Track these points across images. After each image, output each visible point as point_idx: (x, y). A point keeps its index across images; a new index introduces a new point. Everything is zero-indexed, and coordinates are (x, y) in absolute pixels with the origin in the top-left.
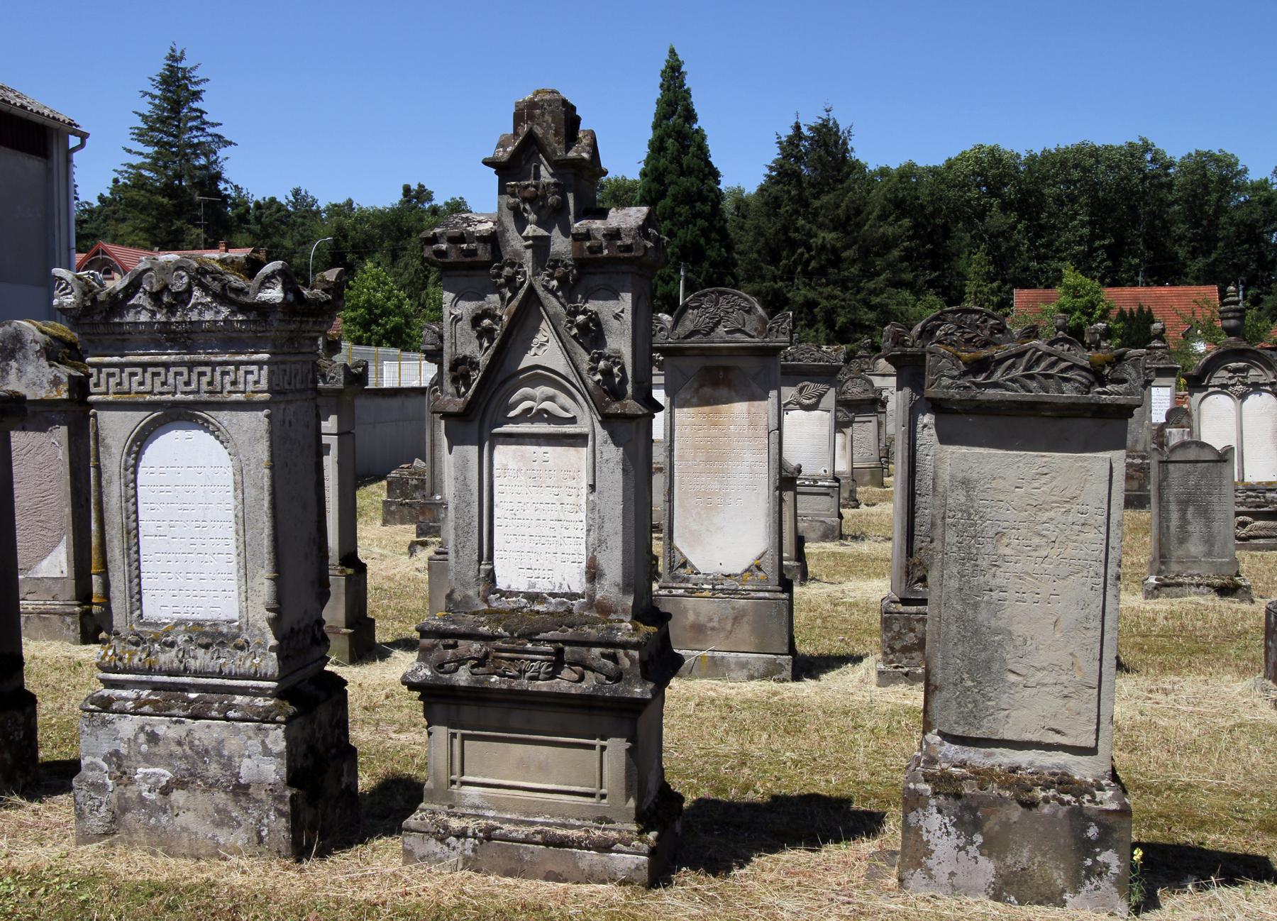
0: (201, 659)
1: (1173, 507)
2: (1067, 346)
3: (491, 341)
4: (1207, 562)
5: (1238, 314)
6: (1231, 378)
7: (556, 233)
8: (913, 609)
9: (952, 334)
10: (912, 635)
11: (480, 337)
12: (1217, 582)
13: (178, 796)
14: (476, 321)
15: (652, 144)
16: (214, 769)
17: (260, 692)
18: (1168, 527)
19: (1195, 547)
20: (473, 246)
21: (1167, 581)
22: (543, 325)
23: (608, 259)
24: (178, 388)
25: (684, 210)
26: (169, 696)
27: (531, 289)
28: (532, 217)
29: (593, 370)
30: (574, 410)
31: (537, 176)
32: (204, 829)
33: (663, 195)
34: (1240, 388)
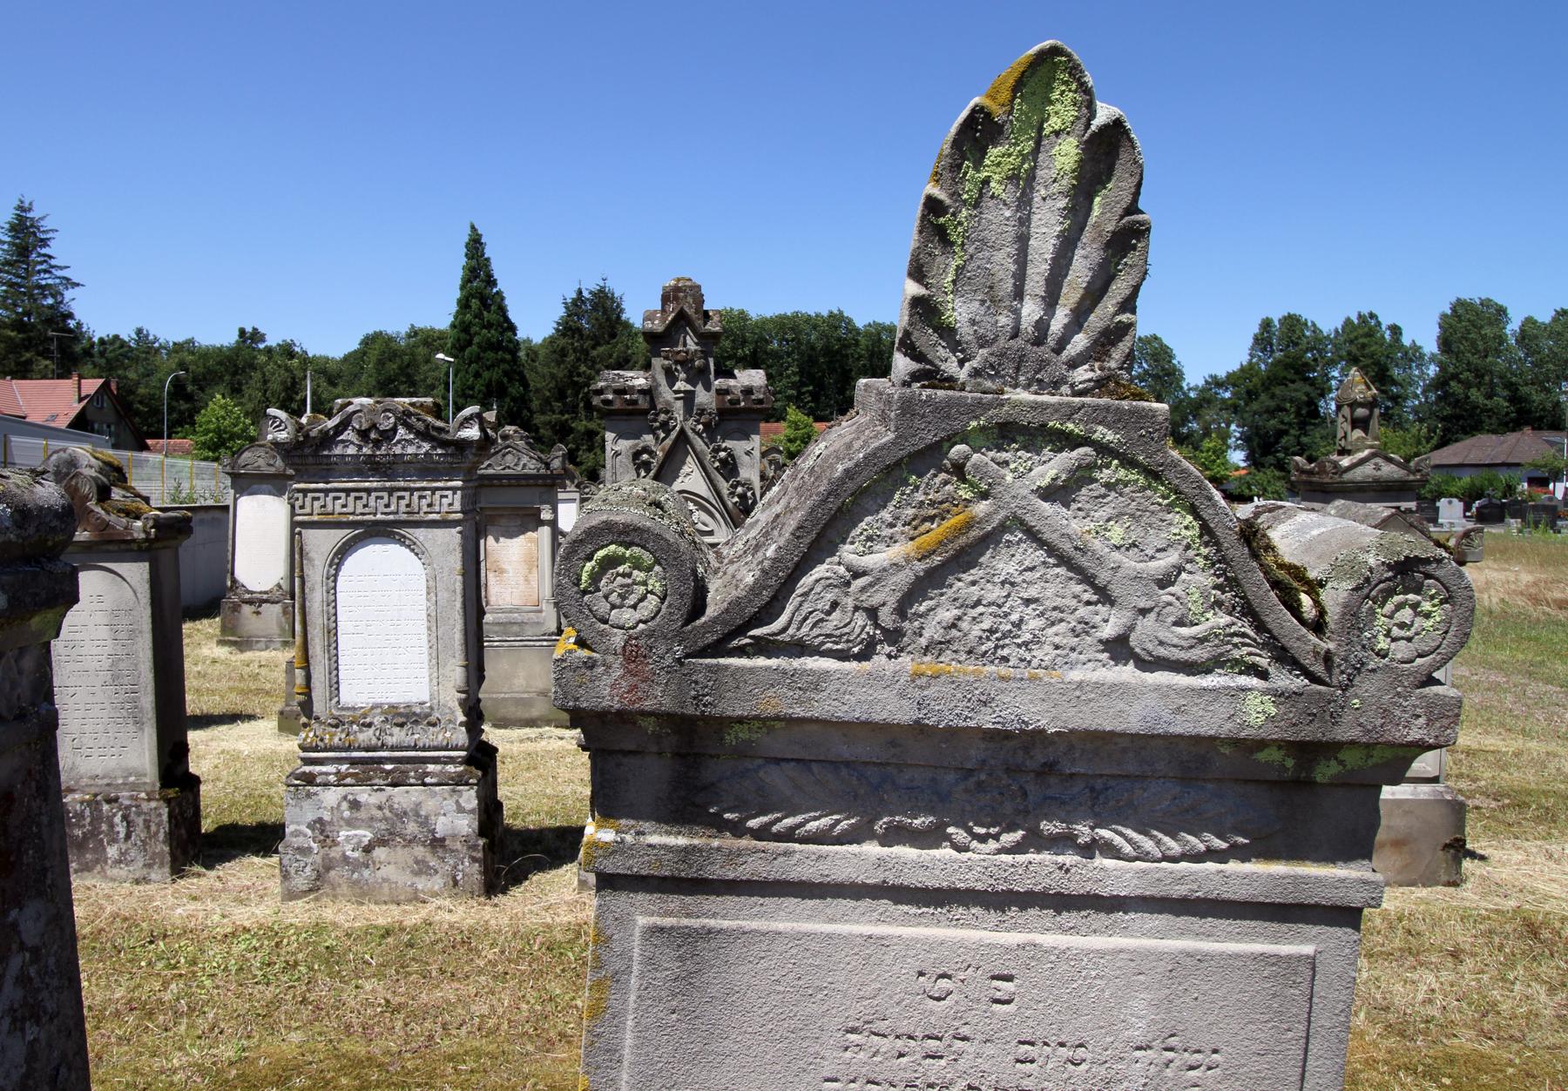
0: (397, 736)
3: (648, 471)
7: (700, 388)
11: (637, 470)
13: (380, 853)
14: (636, 455)
15: (459, 301)
16: (412, 828)
17: (452, 760)
20: (635, 396)
22: (689, 459)
23: (743, 409)
24: (379, 509)
25: (490, 355)
26: (366, 769)
27: (682, 431)
28: (683, 375)
29: (732, 494)
30: (712, 525)
31: (685, 344)
32: (403, 879)
33: (470, 343)
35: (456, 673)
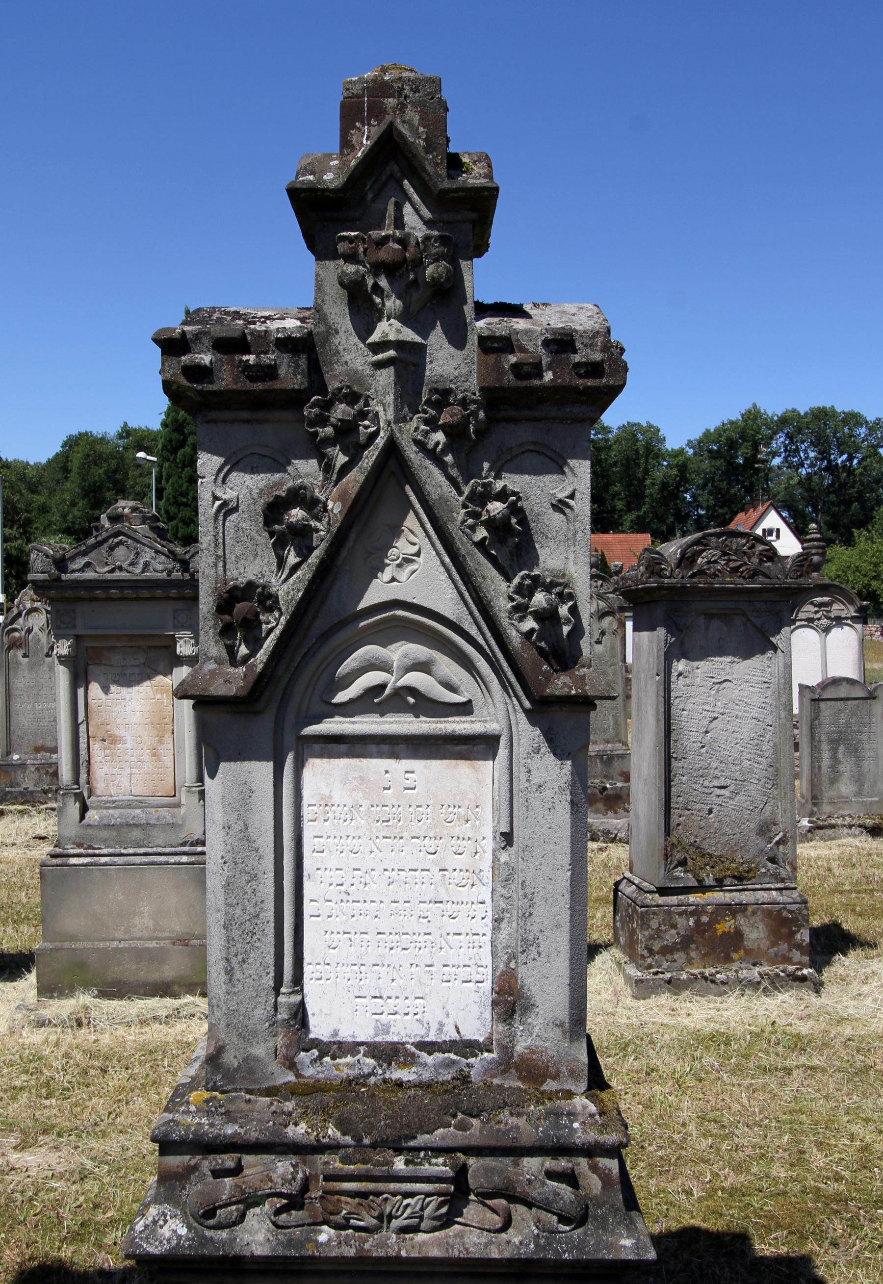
1: (825, 747)
2: (600, 582)
3: (305, 552)
4: (856, 802)
5: (820, 551)
6: (816, 612)
7: (437, 339)
8: (673, 899)
9: (716, 562)
10: (674, 931)
11: (279, 546)
12: (869, 822)
14: (274, 511)
18: (820, 767)
19: (846, 788)
20: (269, 358)
21: (821, 823)
22: (410, 521)
23: (552, 389)
27: (392, 448)
28: (393, 304)
29: (521, 610)
30: (469, 689)
31: (399, 223)
34: (824, 621)
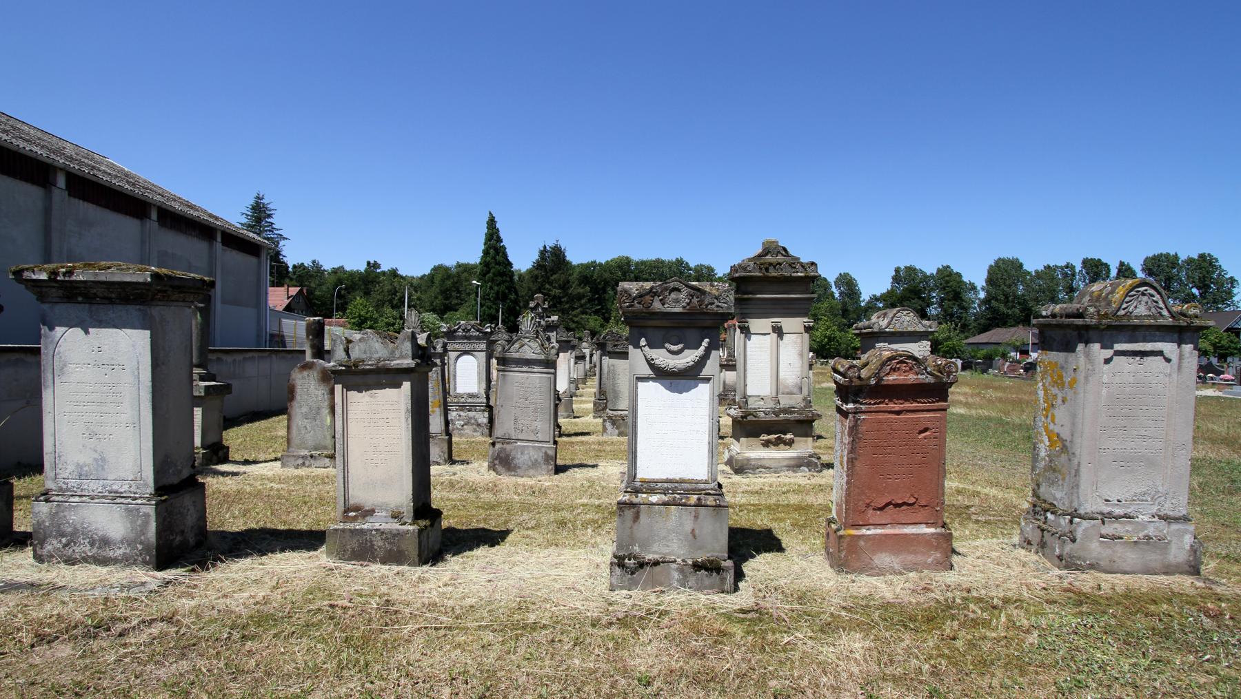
25: (499, 278)
26: (463, 407)
35: (484, 386)
